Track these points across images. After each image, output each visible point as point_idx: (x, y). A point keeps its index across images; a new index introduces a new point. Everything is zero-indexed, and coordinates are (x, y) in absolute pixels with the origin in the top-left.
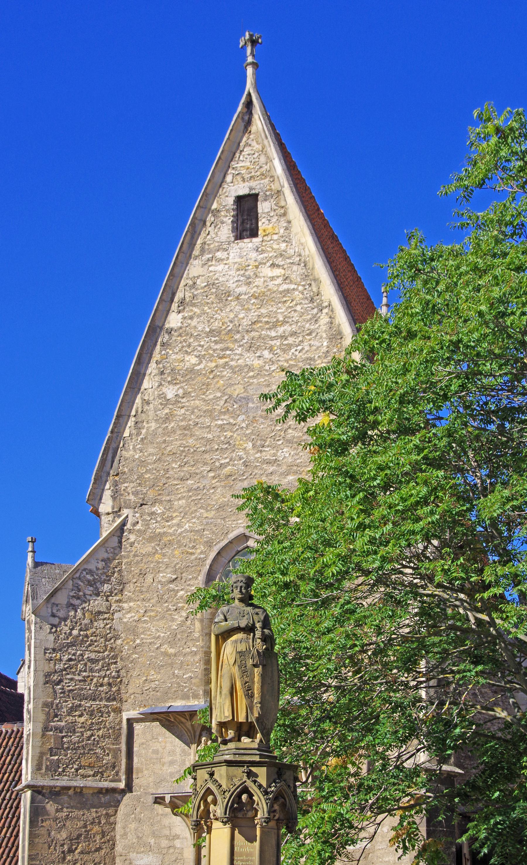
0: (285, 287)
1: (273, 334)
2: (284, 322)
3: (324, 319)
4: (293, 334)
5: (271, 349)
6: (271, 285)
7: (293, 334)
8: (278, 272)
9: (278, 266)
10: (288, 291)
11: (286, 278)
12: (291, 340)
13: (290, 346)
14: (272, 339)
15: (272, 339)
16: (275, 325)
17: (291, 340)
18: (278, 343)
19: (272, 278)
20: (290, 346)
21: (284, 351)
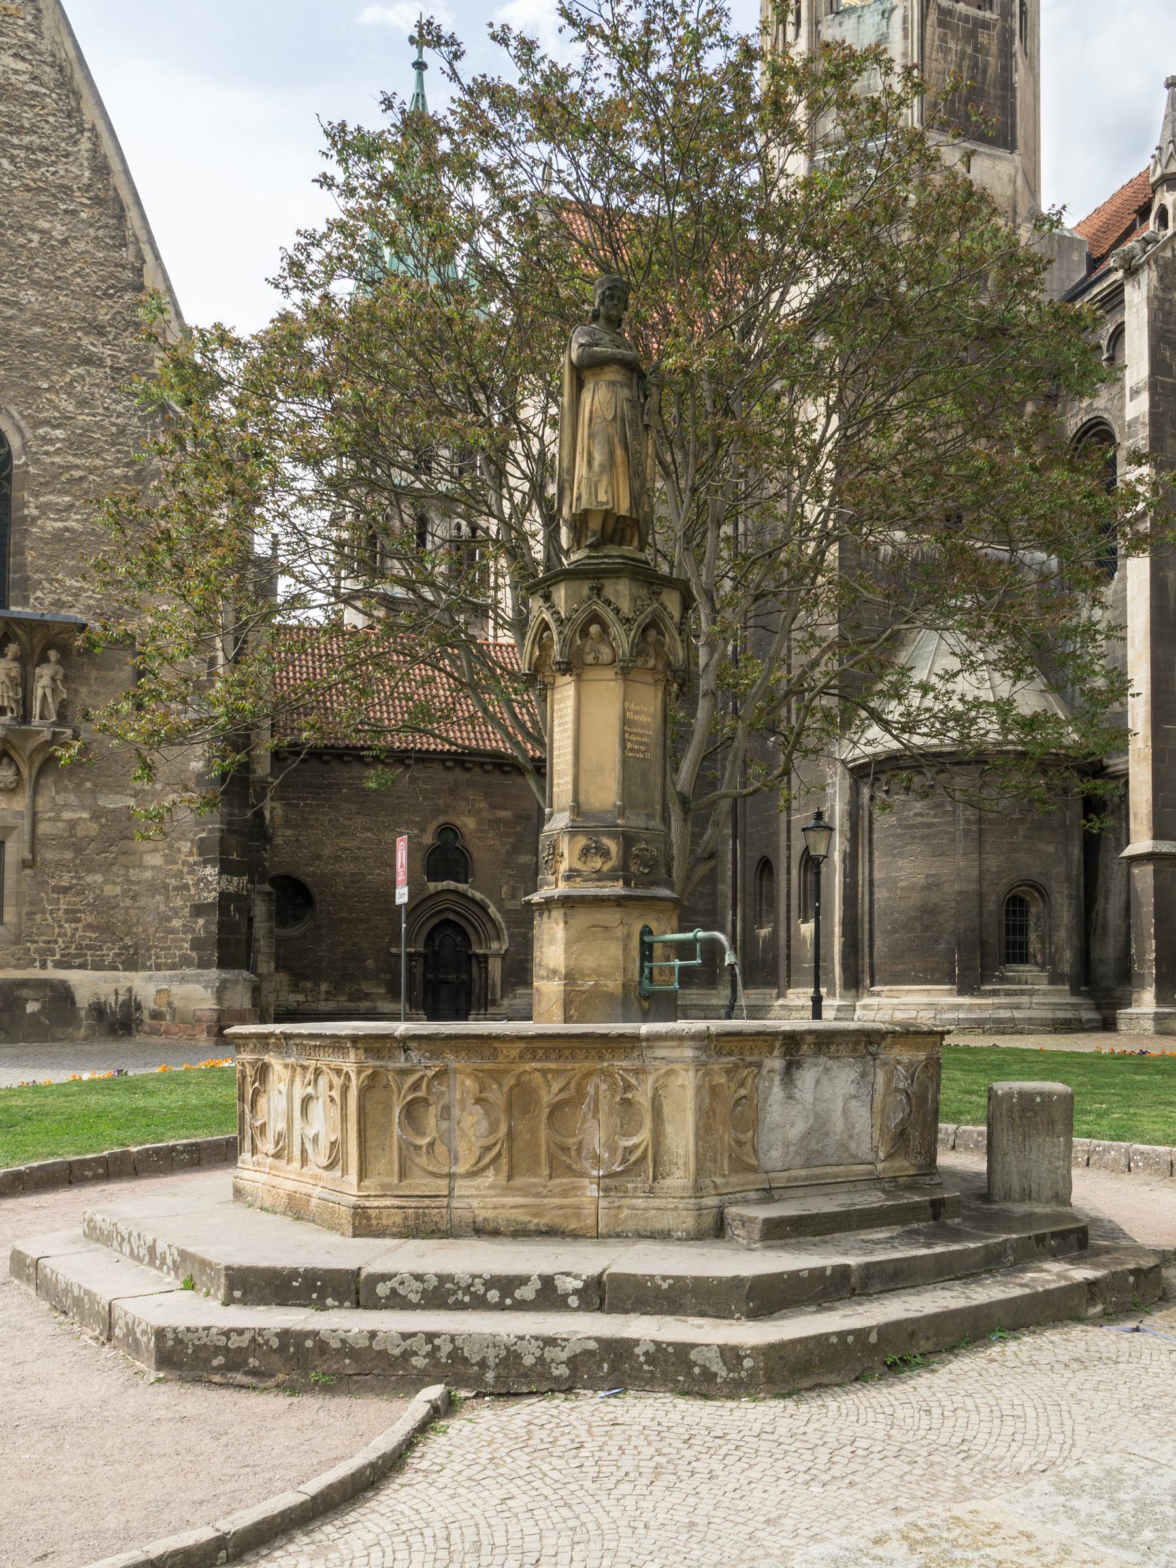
0: (33, 87)
1: (16, 141)
2: (31, 131)
3: (85, 144)
4: (44, 149)
5: (12, 158)
6: (13, 78)
7: (44, 149)
8: (21, 66)
9: (23, 59)
10: (35, 94)
11: (34, 78)
12: (40, 156)
13: (38, 164)
14: (14, 146)
15: (14, 146)
16: (18, 131)
17: (40, 156)
18: (22, 154)
19: (16, 72)
20: (38, 164)
21: (31, 167)
